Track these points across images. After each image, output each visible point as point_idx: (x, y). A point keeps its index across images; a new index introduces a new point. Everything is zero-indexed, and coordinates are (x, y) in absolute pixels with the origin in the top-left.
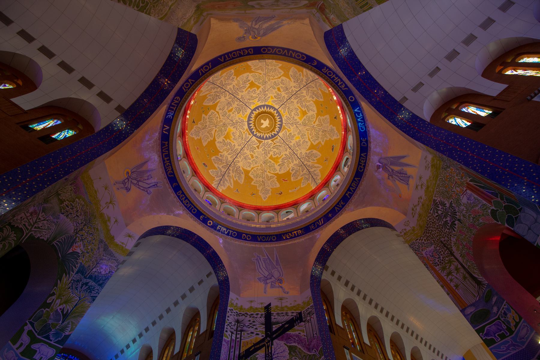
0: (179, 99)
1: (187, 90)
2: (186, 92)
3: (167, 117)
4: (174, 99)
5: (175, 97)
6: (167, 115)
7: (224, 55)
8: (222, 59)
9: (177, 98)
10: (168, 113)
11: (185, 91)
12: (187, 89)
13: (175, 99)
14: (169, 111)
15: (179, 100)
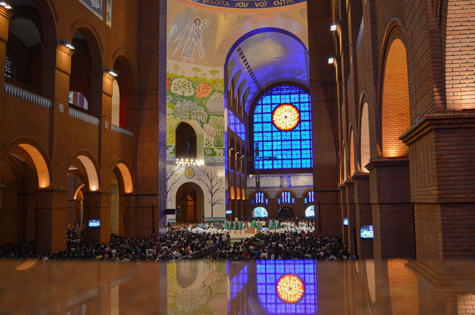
0: (275, 2)
1: (265, 2)
2: (266, 1)
3: (294, 2)
4: (277, 6)
5: (275, 6)
6: (292, 3)
7: (224, 6)
8: (227, 4)
9: (276, 4)
10: (290, 3)
11: (267, 2)
12: (265, 2)
13: (276, 5)
14: (288, 3)
15: (276, 1)
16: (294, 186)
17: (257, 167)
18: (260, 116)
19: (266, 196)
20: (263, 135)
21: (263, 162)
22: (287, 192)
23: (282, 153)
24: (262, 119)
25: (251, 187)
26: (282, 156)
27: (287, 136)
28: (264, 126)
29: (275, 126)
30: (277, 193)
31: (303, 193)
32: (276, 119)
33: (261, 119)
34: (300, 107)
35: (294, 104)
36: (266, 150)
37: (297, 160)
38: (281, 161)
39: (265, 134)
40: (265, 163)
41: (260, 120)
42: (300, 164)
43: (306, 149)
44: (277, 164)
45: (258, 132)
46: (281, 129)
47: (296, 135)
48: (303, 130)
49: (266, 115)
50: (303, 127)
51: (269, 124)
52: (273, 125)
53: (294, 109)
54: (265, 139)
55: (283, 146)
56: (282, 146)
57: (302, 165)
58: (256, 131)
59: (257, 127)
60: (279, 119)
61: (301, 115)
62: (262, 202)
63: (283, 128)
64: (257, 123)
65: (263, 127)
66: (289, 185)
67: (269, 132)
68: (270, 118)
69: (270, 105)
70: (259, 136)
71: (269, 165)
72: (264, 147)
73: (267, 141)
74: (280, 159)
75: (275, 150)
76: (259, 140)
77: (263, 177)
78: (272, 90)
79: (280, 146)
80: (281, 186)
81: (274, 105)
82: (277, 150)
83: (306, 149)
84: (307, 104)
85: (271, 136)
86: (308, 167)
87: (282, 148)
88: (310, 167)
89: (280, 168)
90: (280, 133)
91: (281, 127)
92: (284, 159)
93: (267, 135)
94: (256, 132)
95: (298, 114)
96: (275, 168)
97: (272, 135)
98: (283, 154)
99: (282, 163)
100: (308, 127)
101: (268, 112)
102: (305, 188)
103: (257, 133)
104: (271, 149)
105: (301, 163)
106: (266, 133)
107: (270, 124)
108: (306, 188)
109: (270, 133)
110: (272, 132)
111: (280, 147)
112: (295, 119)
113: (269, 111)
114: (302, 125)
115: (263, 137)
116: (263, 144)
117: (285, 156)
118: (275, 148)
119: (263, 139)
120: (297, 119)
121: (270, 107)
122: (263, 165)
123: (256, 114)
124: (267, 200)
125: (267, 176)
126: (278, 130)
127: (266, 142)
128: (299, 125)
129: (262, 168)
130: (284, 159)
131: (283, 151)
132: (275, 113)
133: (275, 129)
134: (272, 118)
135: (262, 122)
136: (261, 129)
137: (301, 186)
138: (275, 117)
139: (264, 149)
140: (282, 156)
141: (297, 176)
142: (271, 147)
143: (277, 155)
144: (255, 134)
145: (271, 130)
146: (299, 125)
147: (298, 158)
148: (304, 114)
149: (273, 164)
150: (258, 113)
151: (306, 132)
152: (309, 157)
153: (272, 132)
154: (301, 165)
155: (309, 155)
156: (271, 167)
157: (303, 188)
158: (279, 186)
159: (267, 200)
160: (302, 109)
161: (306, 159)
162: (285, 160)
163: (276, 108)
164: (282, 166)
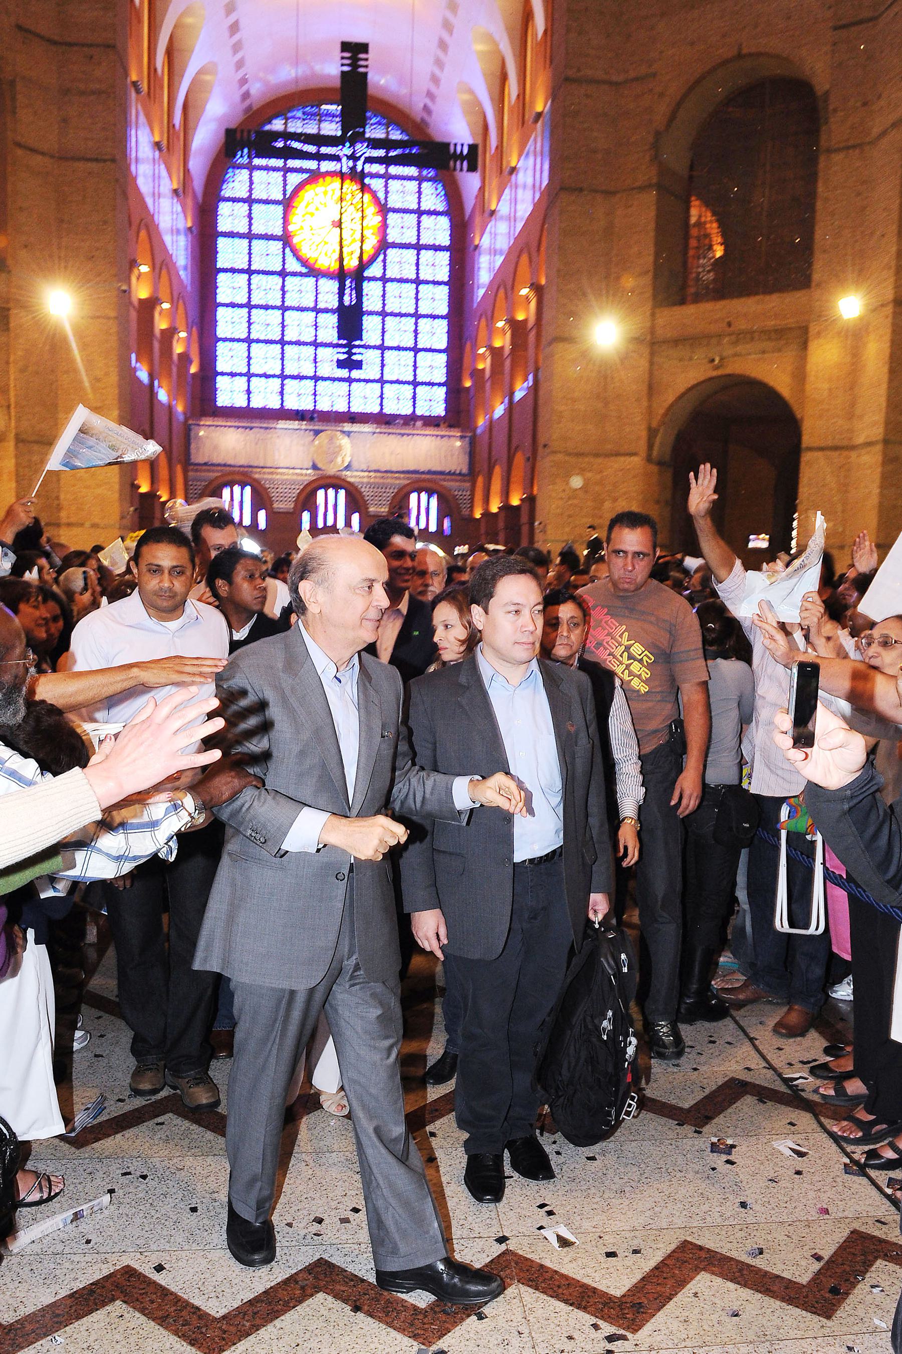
22: (337, 488)
25: (205, 464)
29: (295, 252)
30: (302, 490)
46: (317, 266)
70: (236, 285)
78: (290, 115)
80: (315, 467)
102: (399, 478)
107: (280, 244)
125: (266, 428)
126: (304, 270)
128: (381, 257)
132: (294, 204)
133: (293, 265)
137: (386, 472)
148: (400, 220)
153: (283, 274)
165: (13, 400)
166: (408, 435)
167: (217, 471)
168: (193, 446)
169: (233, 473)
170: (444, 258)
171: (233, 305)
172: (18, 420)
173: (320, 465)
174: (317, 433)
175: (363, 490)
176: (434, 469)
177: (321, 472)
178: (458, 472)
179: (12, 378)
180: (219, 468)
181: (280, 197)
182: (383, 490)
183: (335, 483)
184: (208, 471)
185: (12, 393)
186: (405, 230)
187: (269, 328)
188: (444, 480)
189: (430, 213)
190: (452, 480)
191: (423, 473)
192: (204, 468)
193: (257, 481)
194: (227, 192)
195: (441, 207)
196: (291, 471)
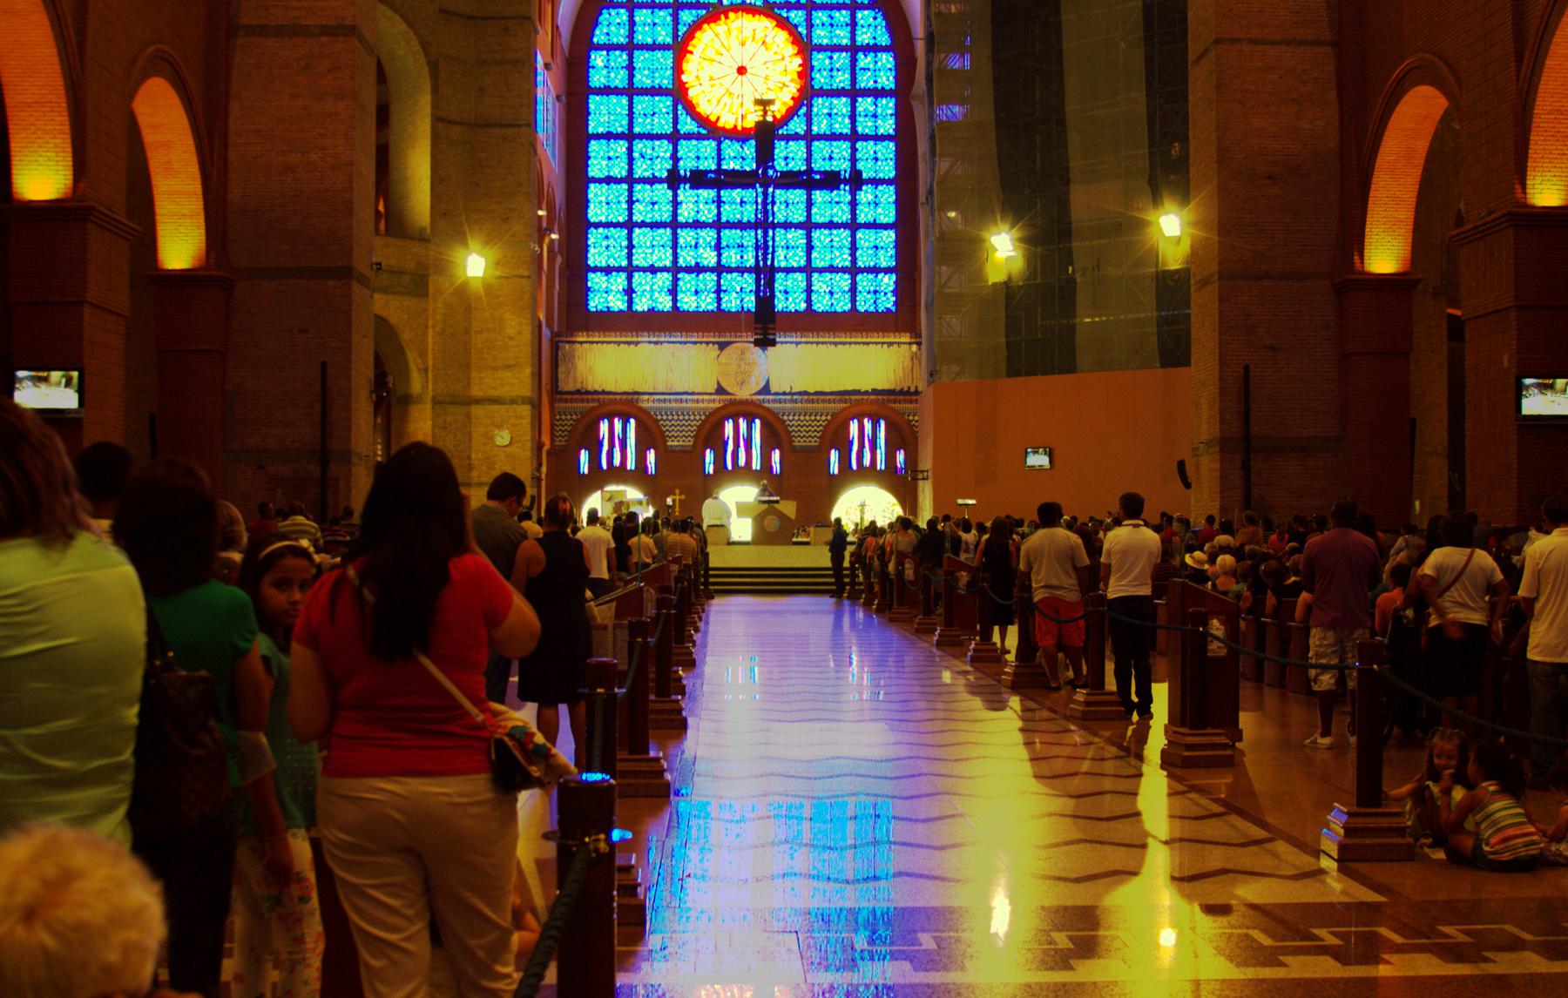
16: (784, 393)
17: (596, 303)
18: (621, 58)
19: (650, 435)
20: (630, 150)
21: (630, 279)
23: (719, 238)
24: (631, 77)
25: (578, 392)
26: (719, 255)
27: (743, 159)
28: (638, 108)
30: (704, 422)
31: (825, 427)
32: (697, 77)
33: (624, 73)
34: (810, 26)
35: (784, 14)
36: (643, 225)
37: (791, 275)
38: (714, 277)
39: (641, 145)
40: (640, 284)
41: (620, 80)
42: (804, 296)
43: (831, 225)
44: (697, 292)
45: (609, 136)
46: (720, 124)
47: (786, 158)
48: (819, 137)
49: (647, 54)
50: (821, 122)
51: (664, 98)
52: (680, 107)
53: (783, 35)
54: (641, 170)
55: (726, 206)
56: (719, 208)
57: (814, 297)
58: (601, 130)
59: (604, 114)
60: (711, 79)
61: (815, 63)
62: (631, 465)
63: (727, 122)
64: (606, 91)
65: (631, 114)
66: (762, 384)
67: (659, 137)
68: (669, 72)
69: (671, 11)
70: (611, 154)
71: (656, 295)
72: (637, 206)
73: (652, 181)
74: (712, 270)
75: (686, 225)
76: (612, 174)
77: (637, 343)
79: (714, 207)
80: (720, 390)
81: (687, 12)
82: (697, 225)
83: (831, 225)
84: (844, 12)
85: (668, 155)
86: (839, 309)
87: (719, 214)
88: (848, 307)
89: (710, 308)
90: (714, 144)
91: (718, 119)
92: (730, 270)
93: (649, 151)
94: (598, 137)
95: (799, 60)
96: (686, 308)
97: (675, 150)
98: (724, 244)
99: (719, 285)
100: (847, 121)
101: (660, 40)
103: (604, 142)
104: (666, 217)
105: (809, 290)
106: (648, 143)
107: (668, 101)
108: (840, 401)
109: (665, 142)
110: (675, 137)
111: (709, 211)
112: (786, 80)
113: (664, 36)
114: (815, 110)
115: (631, 160)
116: (630, 191)
117: (733, 252)
118: (686, 214)
119: (631, 170)
120: (792, 80)
121: (669, 19)
122: (629, 292)
123: (600, 47)
124: (651, 456)
126: (703, 132)
127: (648, 187)
128: (803, 110)
129: (624, 307)
130: (730, 270)
131: (726, 233)
132: (690, 48)
133: (688, 126)
134: (678, 70)
135: (631, 91)
136: (625, 122)
137: (817, 393)
138: (690, 66)
139: (637, 218)
140: (719, 255)
141: (797, 343)
142: (669, 207)
143: (696, 247)
144: (593, 142)
145: (668, 129)
146: (803, 110)
147: (795, 265)
148: (827, 61)
149: (673, 292)
150: (609, 48)
151: (834, 143)
152: (848, 264)
153: (675, 137)
154: (809, 301)
155: (848, 252)
156: (665, 304)
157: (824, 401)
158: (712, 388)
159: (651, 456)
160: (819, 36)
161: (832, 269)
162: (735, 275)
163: (696, 27)
164: (719, 300)
165: (430, 363)
166: (844, 343)
167: (593, 400)
168: (561, 369)
169: (614, 402)
170: (888, 105)
171: (609, 180)
172: (435, 382)
173: (729, 389)
174: (723, 346)
175: (785, 418)
176: (880, 388)
177: (728, 397)
178: (912, 389)
179: (430, 340)
180: (595, 397)
181: (669, 40)
182: (813, 418)
183: (748, 410)
184: (582, 401)
185: (430, 356)
186: (835, 73)
187: (656, 207)
188: (895, 401)
189: (867, 49)
190: (906, 401)
191: (866, 393)
192: (576, 397)
193: (641, 409)
194: (599, 37)
195: (884, 40)
196: (689, 397)
